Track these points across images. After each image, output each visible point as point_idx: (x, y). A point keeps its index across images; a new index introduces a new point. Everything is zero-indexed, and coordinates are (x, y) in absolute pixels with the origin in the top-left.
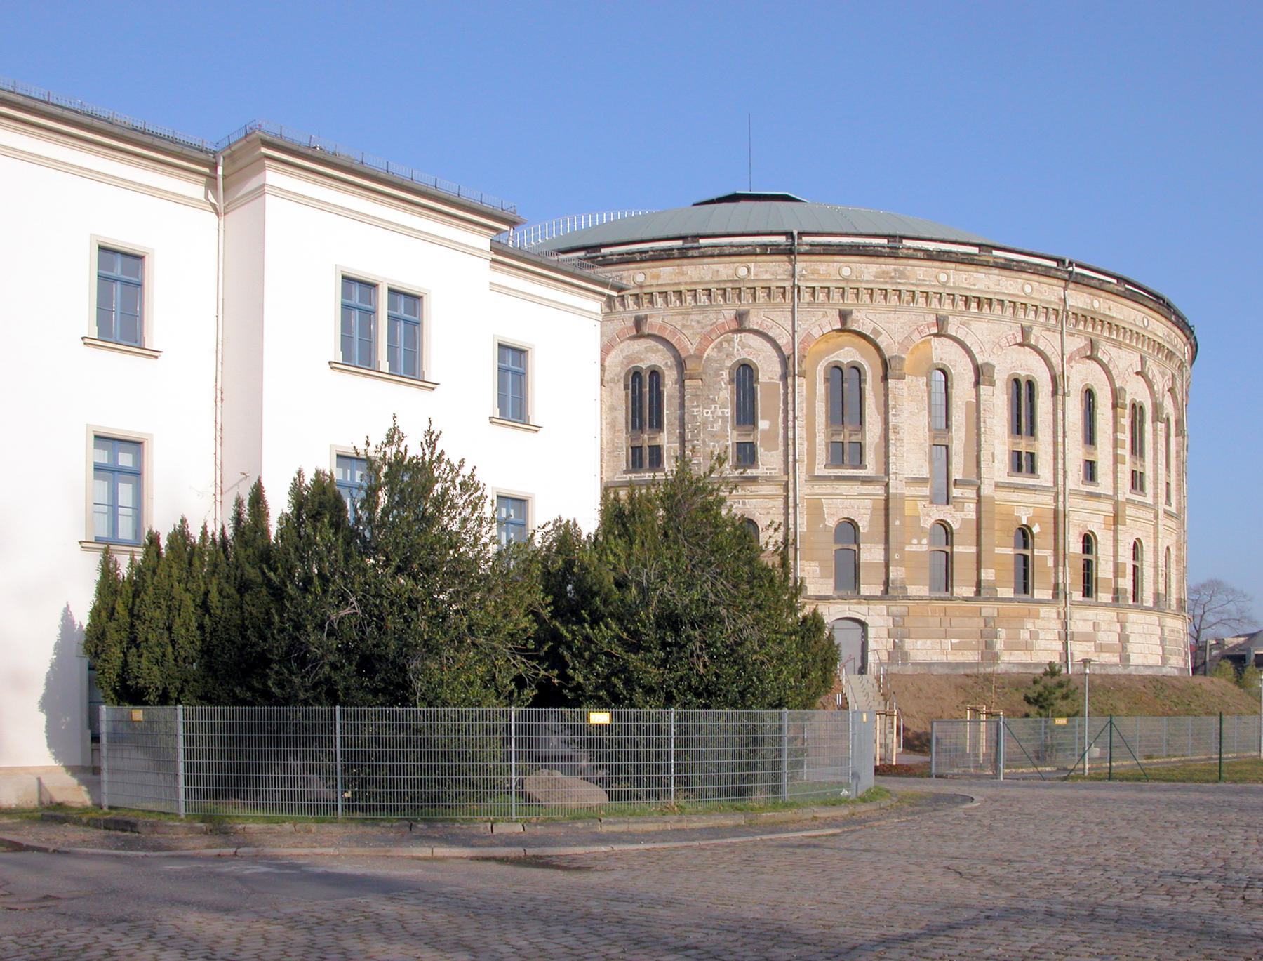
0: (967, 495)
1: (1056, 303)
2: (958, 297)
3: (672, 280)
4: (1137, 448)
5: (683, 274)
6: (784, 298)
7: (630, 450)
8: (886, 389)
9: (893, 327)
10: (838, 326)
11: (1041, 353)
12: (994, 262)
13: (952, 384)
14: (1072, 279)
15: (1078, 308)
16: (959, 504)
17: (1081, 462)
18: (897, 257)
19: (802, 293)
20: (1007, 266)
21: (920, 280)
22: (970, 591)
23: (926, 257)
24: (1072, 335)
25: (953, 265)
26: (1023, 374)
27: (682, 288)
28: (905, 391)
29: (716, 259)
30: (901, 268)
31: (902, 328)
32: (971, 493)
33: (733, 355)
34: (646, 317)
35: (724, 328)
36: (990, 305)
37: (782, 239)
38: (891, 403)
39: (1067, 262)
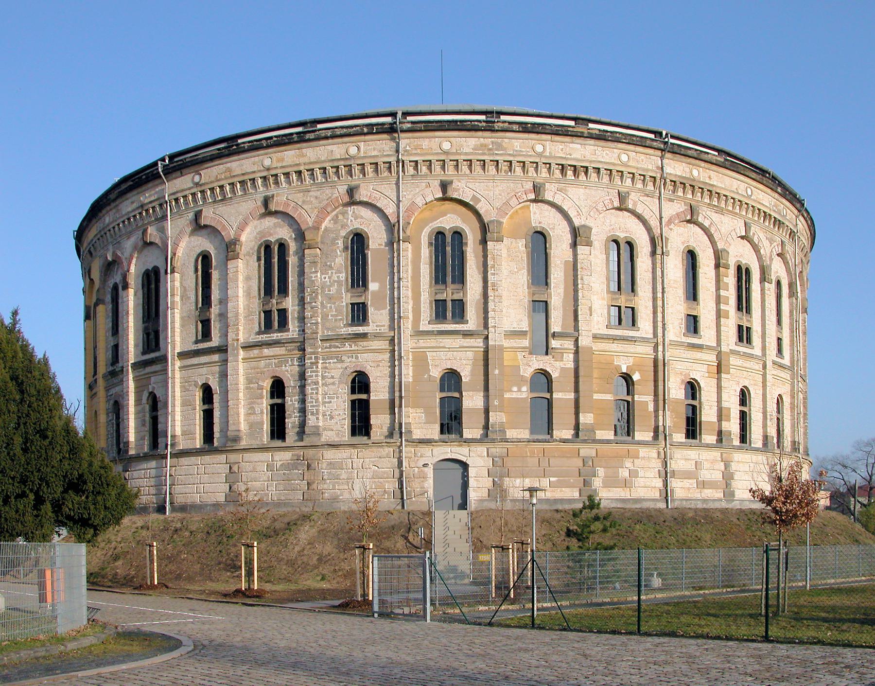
0: (566, 346)
1: (652, 171)
2: (553, 166)
3: (293, 161)
4: (743, 304)
5: (303, 156)
6: (391, 172)
7: (263, 315)
9: (491, 194)
10: (440, 195)
11: (639, 217)
12: (588, 133)
13: (551, 245)
14: (668, 149)
15: (676, 175)
16: (559, 355)
17: (683, 316)
18: (493, 130)
19: (406, 166)
20: (601, 137)
21: (516, 151)
22: (568, 434)
23: (521, 129)
24: (671, 200)
25: (549, 137)
26: (621, 235)
27: (302, 168)
28: (504, 253)
29: (330, 141)
30: (499, 140)
31: (500, 195)
33: (347, 225)
34: (273, 196)
35: (338, 201)
36: (586, 173)
37: (389, 119)
38: (490, 262)
39: (664, 134)
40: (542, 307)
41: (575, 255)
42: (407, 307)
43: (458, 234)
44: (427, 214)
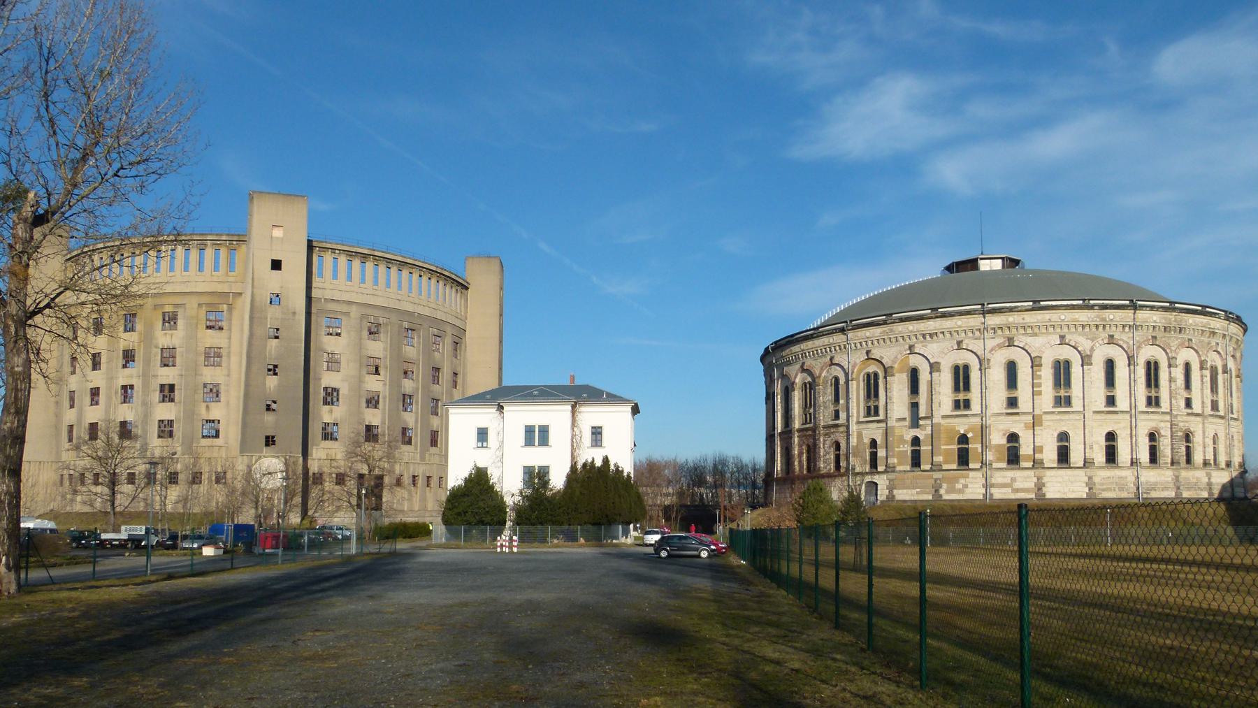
5: (814, 344)
8: (886, 381)
26: (961, 362)
27: (813, 349)
32: (929, 422)
38: (888, 387)
40: (915, 406)
41: (932, 377)
42: (853, 411)
43: (876, 375)
44: (863, 366)
